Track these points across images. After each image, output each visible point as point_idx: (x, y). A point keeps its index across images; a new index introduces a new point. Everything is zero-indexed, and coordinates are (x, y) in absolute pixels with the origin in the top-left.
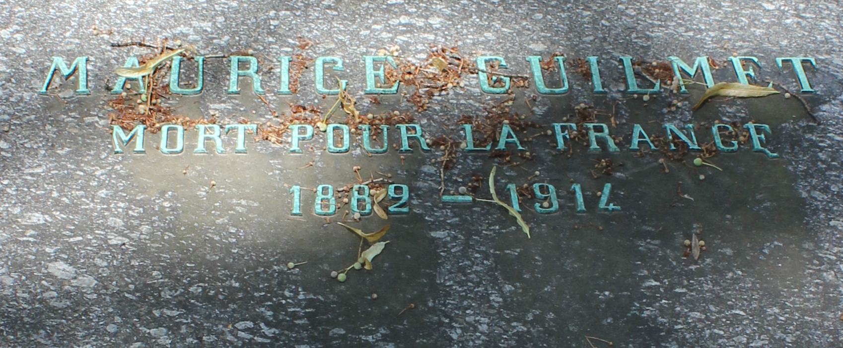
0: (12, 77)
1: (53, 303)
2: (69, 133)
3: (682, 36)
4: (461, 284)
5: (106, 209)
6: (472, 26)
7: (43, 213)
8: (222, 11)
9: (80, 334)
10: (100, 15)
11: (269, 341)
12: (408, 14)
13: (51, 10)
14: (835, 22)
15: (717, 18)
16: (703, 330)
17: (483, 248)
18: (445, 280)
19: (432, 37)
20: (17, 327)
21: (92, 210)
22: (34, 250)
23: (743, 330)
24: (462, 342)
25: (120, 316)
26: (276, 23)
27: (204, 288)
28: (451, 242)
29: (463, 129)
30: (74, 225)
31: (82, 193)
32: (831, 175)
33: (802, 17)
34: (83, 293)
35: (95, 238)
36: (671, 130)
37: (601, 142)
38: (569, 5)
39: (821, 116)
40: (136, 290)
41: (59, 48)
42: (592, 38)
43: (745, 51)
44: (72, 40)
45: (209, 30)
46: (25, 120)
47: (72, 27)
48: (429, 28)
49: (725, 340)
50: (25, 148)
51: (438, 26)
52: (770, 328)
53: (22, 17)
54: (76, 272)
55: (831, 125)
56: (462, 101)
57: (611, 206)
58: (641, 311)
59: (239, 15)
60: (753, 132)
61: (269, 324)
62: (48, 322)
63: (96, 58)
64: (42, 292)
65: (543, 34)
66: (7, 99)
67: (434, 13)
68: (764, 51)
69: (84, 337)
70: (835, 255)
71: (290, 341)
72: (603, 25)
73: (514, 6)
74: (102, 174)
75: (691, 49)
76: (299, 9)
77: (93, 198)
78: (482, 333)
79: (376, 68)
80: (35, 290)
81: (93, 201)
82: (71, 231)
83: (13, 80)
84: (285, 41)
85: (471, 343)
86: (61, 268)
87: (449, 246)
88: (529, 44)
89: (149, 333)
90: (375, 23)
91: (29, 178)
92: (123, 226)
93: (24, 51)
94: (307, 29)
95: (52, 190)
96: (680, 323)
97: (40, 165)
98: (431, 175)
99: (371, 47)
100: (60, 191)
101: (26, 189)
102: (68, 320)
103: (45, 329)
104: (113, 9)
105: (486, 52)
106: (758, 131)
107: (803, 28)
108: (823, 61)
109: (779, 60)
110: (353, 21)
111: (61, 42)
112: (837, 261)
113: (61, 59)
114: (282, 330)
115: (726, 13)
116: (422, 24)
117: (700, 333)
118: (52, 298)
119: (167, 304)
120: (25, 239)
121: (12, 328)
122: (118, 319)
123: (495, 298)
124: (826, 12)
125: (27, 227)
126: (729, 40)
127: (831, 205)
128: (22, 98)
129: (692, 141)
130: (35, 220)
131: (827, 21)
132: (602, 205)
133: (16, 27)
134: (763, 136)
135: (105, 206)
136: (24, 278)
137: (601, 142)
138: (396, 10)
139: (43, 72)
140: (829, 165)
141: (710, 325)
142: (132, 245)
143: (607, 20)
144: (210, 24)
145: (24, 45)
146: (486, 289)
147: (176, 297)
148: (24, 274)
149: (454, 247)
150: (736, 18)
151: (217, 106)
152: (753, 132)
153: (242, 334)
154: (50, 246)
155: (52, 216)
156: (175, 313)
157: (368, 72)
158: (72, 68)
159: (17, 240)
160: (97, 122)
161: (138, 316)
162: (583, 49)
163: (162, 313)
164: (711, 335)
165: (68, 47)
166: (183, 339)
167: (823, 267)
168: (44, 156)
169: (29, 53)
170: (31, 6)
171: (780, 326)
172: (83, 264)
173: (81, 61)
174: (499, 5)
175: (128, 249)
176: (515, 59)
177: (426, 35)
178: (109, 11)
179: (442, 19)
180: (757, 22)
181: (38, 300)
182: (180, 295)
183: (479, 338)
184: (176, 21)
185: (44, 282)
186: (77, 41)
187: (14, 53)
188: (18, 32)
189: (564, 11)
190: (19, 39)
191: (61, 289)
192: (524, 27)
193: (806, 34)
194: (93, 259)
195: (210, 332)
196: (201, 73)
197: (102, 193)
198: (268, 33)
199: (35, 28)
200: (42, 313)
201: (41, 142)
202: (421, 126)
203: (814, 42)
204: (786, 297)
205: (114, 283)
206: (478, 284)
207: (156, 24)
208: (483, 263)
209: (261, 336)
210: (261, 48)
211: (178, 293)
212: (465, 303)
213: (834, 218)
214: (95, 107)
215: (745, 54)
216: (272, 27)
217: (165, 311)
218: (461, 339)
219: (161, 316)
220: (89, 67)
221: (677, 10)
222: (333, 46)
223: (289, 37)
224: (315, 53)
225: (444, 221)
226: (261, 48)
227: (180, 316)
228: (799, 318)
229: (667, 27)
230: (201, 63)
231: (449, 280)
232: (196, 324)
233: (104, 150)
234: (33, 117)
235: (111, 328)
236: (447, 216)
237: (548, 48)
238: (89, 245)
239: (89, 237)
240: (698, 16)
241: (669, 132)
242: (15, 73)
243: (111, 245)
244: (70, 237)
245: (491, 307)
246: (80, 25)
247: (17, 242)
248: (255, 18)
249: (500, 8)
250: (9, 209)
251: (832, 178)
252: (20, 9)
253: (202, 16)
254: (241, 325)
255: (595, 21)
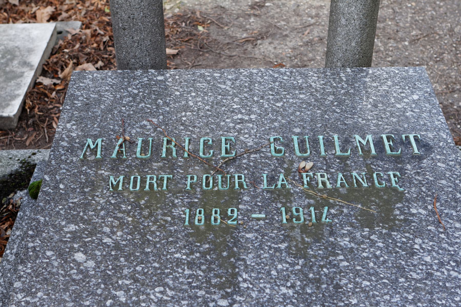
0: (69, 149)
1: (74, 277)
2: (91, 179)
3: (360, 123)
4: (258, 264)
5: (103, 222)
6: (269, 119)
7: (75, 225)
8: (162, 113)
9: (85, 295)
10: (110, 115)
11: (169, 299)
12: (242, 113)
13: (90, 113)
14: (429, 114)
15: (376, 113)
16: (369, 292)
17: (269, 244)
18: (251, 262)
19: (251, 125)
20: (57, 291)
21: (97, 223)
22: (69, 245)
23: (388, 292)
24: (258, 299)
25: (104, 284)
26: (184, 119)
27: (143, 268)
28: (255, 240)
29: (263, 176)
30: (88, 231)
31: (93, 213)
32: (428, 200)
33: (414, 112)
34: (88, 271)
35: (97, 239)
36: (355, 176)
37: (324, 183)
38: (311, 107)
39: (423, 166)
40: (113, 269)
41: (91, 133)
42: (320, 125)
43: (388, 130)
44: (97, 129)
45: (156, 123)
46: (72, 173)
47: (98, 122)
48: (250, 121)
49: (379, 298)
50: (71, 188)
51: (254, 119)
52: (400, 291)
53: (77, 117)
54: (86, 259)
55: (427, 171)
56: (263, 161)
57: (328, 220)
58: (340, 280)
59: (169, 115)
60: (392, 176)
61: (171, 289)
62: (71, 288)
63: (106, 139)
64: (70, 270)
65: (299, 123)
66: (66, 161)
67: (253, 113)
68: (396, 130)
69: (86, 297)
70: (431, 246)
71: (179, 299)
72: (326, 118)
73: (287, 108)
74: (103, 203)
75: (364, 130)
76: (195, 111)
77: (98, 216)
78: (267, 294)
79: (226, 144)
80: (67, 269)
81: (97, 218)
82: (86, 235)
83: (69, 151)
84: (188, 129)
85: (261, 300)
86: (80, 256)
87: (254, 242)
88: (293, 129)
89: (116, 295)
90: (227, 118)
91: (71, 205)
92: (110, 232)
93: (76, 135)
94: (198, 122)
95: (80, 211)
96: (358, 288)
97: (76, 198)
98: (247, 202)
99: (225, 131)
100: (84, 212)
101: (69, 211)
102: (80, 286)
103: (69, 292)
104: (116, 112)
105: (275, 134)
106: (395, 176)
107: (414, 117)
108: (423, 135)
109: (404, 136)
110: (218, 117)
111: (92, 130)
112: (431, 250)
113: (90, 140)
114: (176, 292)
115: (380, 110)
116: (247, 118)
117: (368, 293)
118: (74, 274)
119: (125, 277)
120: (66, 239)
121: (54, 291)
122: (103, 286)
123: (274, 273)
124: (425, 108)
125: (67, 233)
126: (381, 125)
127: (428, 217)
128: (72, 160)
129: (364, 182)
130: (71, 228)
131: (425, 114)
132: (323, 219)
133: (74, 122)
134: (396, 179)
135: (103, 221)
136: (63, 262)
137: (324, 183)
138: (237, 111)
139: (83, 146)
140: (427, 194)
141: (372, 289)
142: (112, 243)
143: (327, 115)
144: (156, 120)
145: (76, 132)
146: (270, 268)
147: (130, 273)
148: (63, 260)
149: (256, 243)
150: (384, 113)
151: (156, 164)
152: (392, 176)
153: (158, 295)
154: (77, 243)
155: (79, 226)
156: (128, 282)
157: (222, 146)
158: (95, 144)
159: (62, 240)
160: (103, 173)
161: (112, 284)
162: (317, 131)
163: (123, 283)
164: (373, 294)
165: (95, 133)
166: (131, 298)
167: (425, 254)
168: (79, 192)
169: (78, 136)
170: (81, 111)
171: (405, 290)
172: (90, 253)
173: (99, 141)
174: (281, 108)
175: (110, 245)
176: (287, 137)
177: (249, 125)
178: (114, 113)
179: (256, 116)
180: (393, 115)
181: (68, 275)
182: (131, 272)
183: (265, 296)
184: (142, 118)
185: (71, 264)
186: (99, 129)
187: (72, 136)
188: (74, 125)
189: (309, 110)
190: (74, 128)
191: (79, 268)
192: (291, 120)
193: (416, 120)
194: (95, 251)
195: (143, 293)
196: (150, 147)
197: (102, 213)
198: (181, 125)
199: (81, 122)
200: (69, 282)
201: (78, 184)
202: (244, 174)
203: (419, 125)
204: (408, 272)
205: (103, 265)
206: (266, 265)
207: (133, 120)
208: (269, 253)
209: (167, 296)
210: (178, 132)
211: (131, 270)
212: (260, 276)
213: (430, 225)
214: (104, 165)
215: (388, 133)
216: (183, 121)
217: (124, 281)
218: (258, 297)
219: (122, 284)
220: (103, 144)
221: (358, 109)
222: (208, 131)
223: (190, 126)
224: (201, 135)
225: (252, 228)
226: (178, 132)
227: (131, 284)
228: (414, 285)
229: (354, 118)
230: (151, 141)
231: (253, 262)
232: (138, 289)
233: (105, 189)
234: (76, 171)
235: (99, 292)
236: (254, 225)
237: (302, 131)
238: (94, 243)
239: (94, 238)
240: (367, 112)
241: (354, 177)
242: (71, 147)
243: (103, 243)
244: (86, 238)
245: (272, 278)
246: (101, 121)
247: (61, 241)
248: (176, 116)
249: (281, 110)
250: (61, 223)
251: (429, 201)
252: (76, 112)
253: (153, 115)
254: (157, 289)
255: (322, 116)
